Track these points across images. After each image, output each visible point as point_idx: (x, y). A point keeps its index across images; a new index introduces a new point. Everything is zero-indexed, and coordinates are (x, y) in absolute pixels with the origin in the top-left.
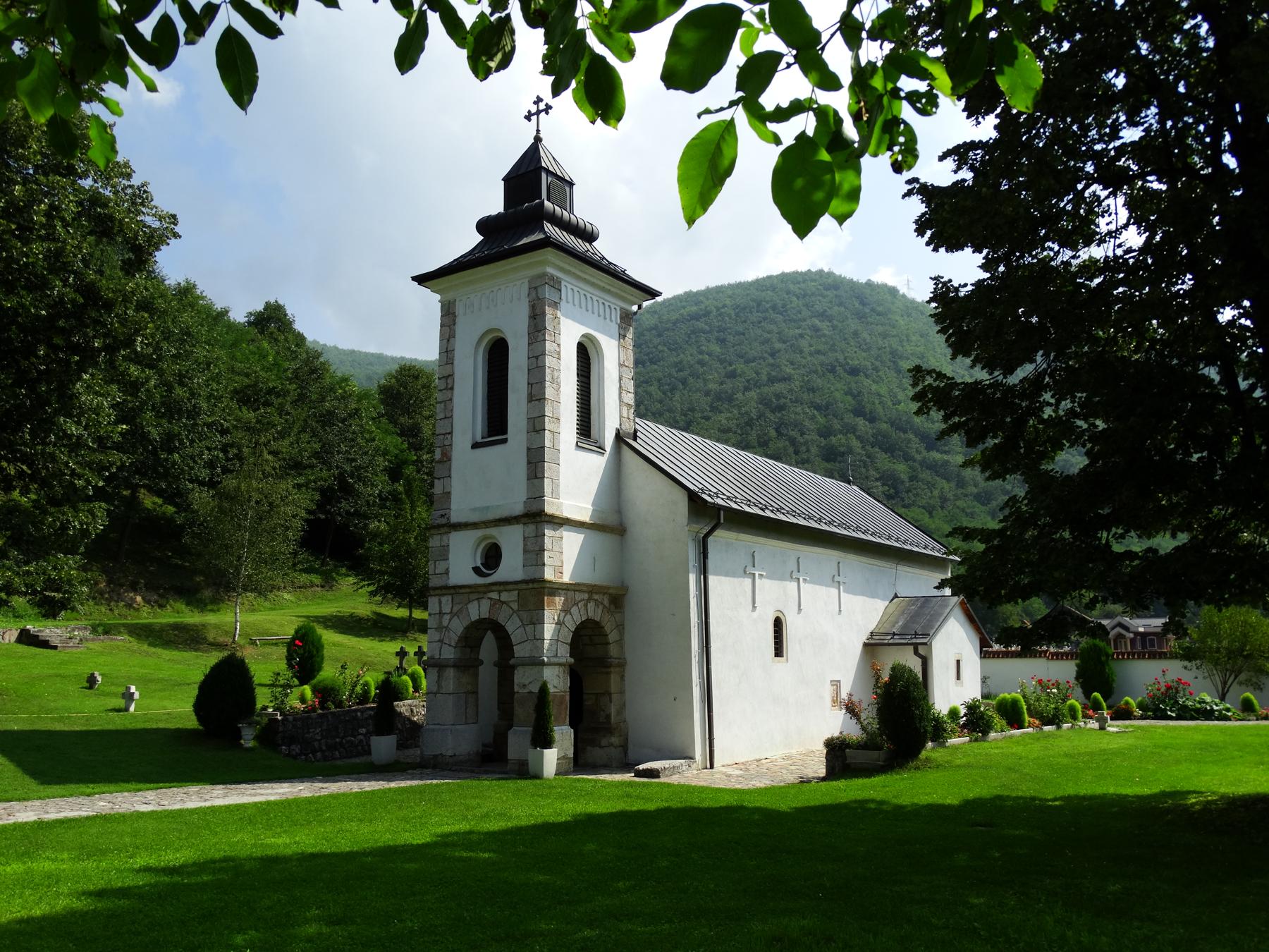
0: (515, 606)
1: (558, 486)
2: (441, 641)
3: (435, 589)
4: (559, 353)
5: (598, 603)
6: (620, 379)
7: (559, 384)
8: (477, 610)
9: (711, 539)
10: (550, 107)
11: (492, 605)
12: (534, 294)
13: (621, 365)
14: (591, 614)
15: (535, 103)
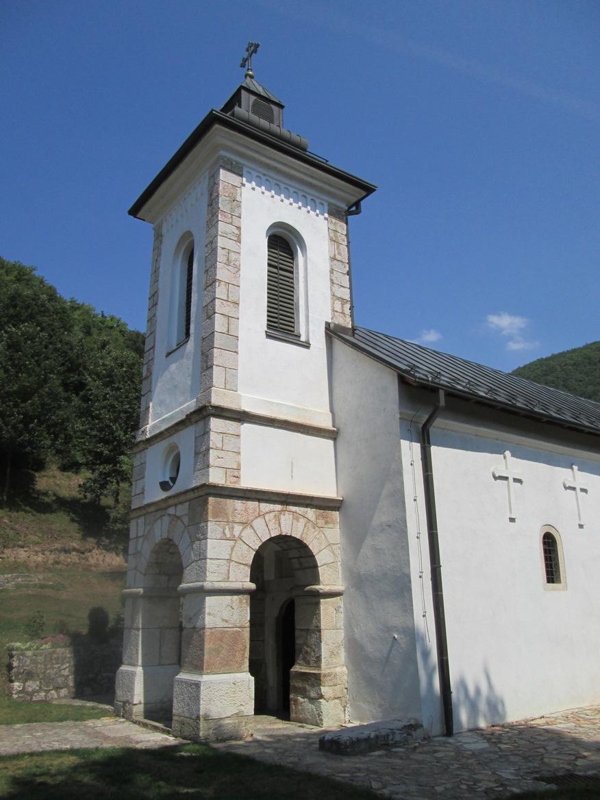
0: (186, 520)
1: (236, 376)
2: (135, 568)
3: (135, 510)
4: (239, 236)
5: (296, 517)
6: (332, 271)
7: (238, 269)
8: (160, 530)
9: (432, 430)
10: (257, 46)
11: (170, 523)
12: (212, 182)
13: (333, 259)
14: (286, 531)
15: (247, 50)
